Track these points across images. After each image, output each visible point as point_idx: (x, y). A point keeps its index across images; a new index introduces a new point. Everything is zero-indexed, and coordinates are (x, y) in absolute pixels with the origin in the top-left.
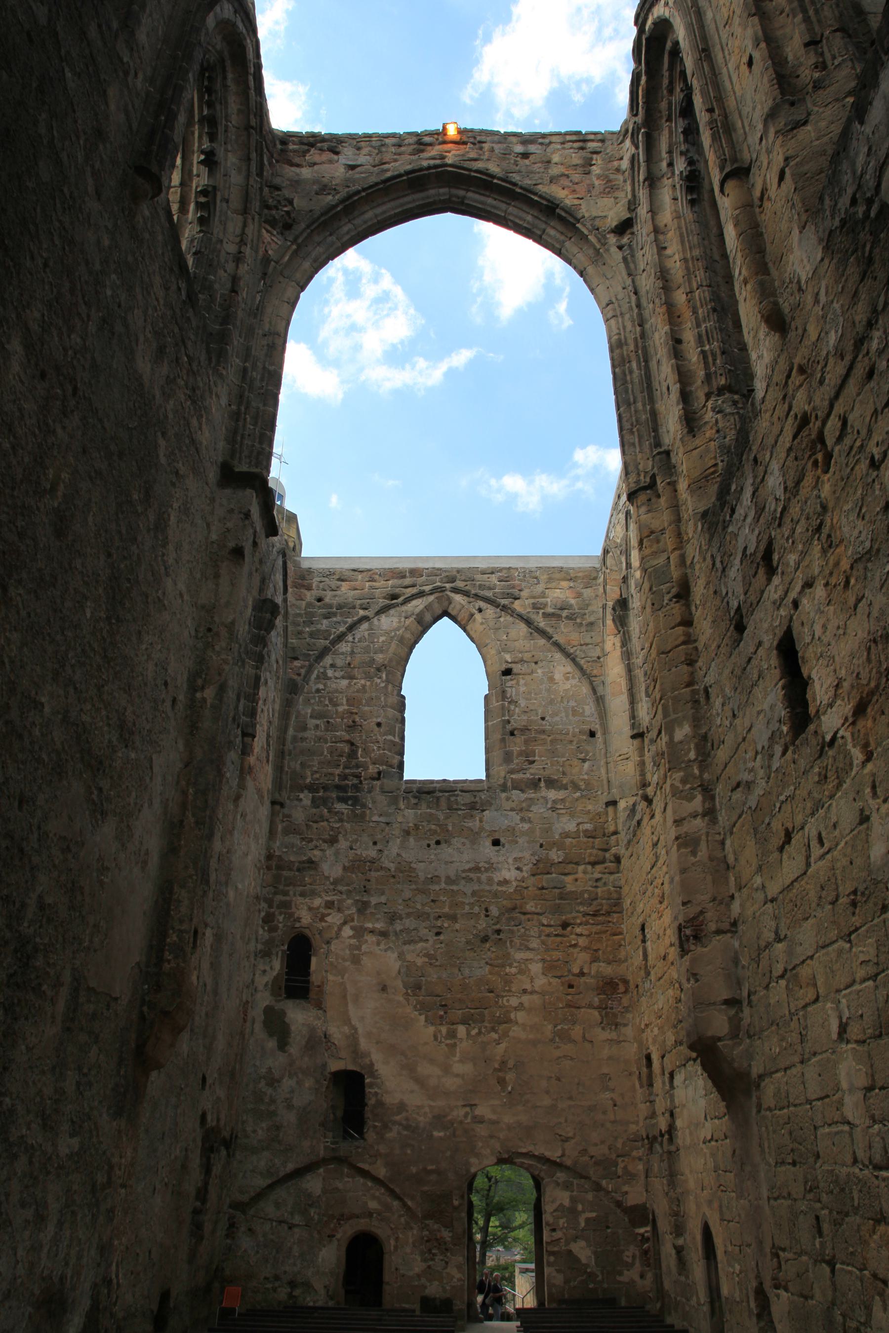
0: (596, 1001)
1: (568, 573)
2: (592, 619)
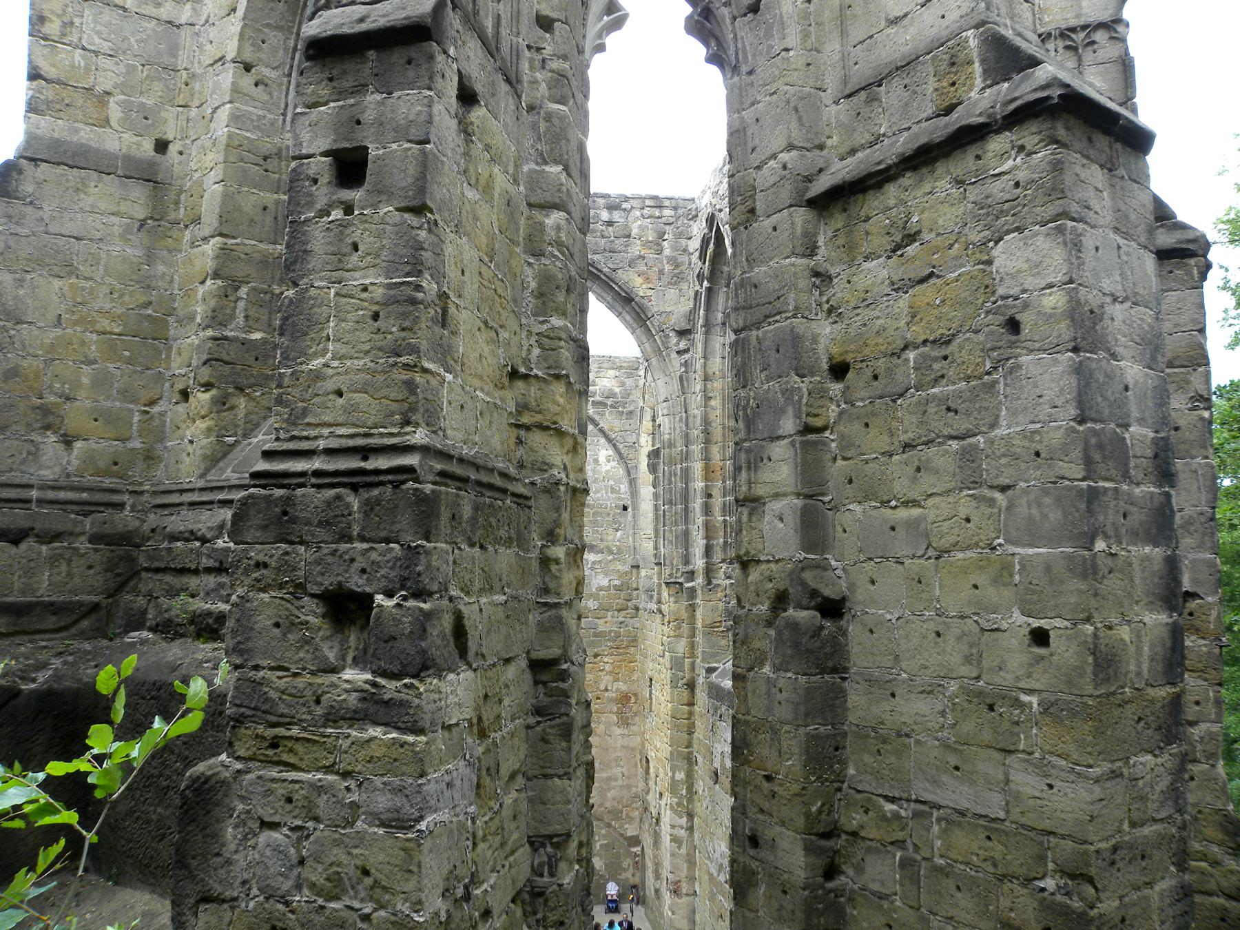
0: (615, 709)
1: (614, 363)
2: (632, 408)
